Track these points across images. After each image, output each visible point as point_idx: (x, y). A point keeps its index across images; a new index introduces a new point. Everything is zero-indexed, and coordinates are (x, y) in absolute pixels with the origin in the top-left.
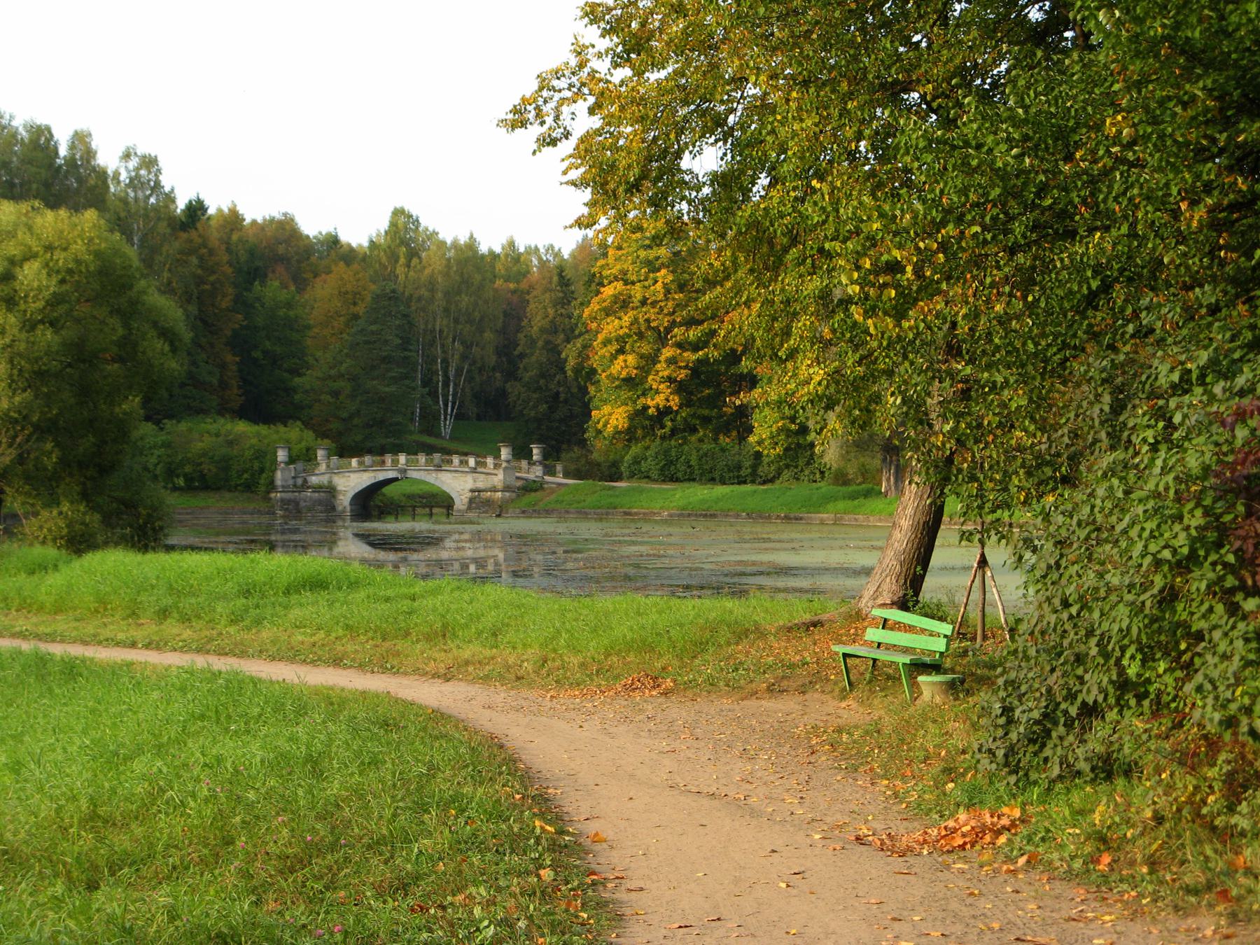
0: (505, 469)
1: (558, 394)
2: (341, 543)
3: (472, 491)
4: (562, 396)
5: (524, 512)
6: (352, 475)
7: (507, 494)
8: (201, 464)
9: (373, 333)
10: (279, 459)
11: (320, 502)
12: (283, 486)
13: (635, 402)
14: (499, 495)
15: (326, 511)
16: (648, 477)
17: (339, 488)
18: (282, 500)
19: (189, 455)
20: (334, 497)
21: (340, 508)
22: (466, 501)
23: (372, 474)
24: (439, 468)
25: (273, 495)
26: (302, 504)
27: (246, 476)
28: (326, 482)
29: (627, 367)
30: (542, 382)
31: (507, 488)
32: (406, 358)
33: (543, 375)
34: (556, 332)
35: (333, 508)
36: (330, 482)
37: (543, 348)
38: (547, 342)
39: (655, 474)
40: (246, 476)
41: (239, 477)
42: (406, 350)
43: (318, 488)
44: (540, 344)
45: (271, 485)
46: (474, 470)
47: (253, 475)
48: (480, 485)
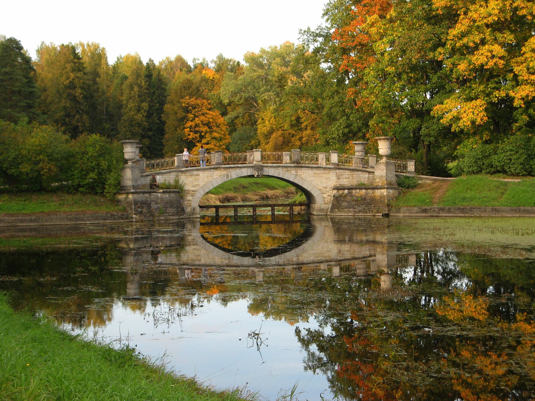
1: (77, 126)
2: (189, 249)
3: (338, 188)
4: (81, 128)
5: (425, 211)
6: (201, 173)
7: (391, 191)
8: (37, 163)
9: (6, 73)
10: (126, 156)
11: (171, 204)
12: (134, 187)
13: (488, 95)
14: (378, 192)
15: (177, 214)
16: (504, 172)
17: (187, 188)
18: (136, 202)
19: (24, 152)
20: (182, 198)
21: (188, 210)
23: (224, 172)
24: (298, 164)
25: (122, 197)
26: (154, 206)
27: (92, 175)
28: (172, 182)
29: (493, 57)
30: (67, 119)
31: (390, 186)
32: (31, 93)
33: (68, 115)
34: (75, 88)
35: (183, 210)
36: (177, 181)
37: (66, 98)
38: (69, 95)
39: (516, 167)
40: (92, 175)
41: (84, 177)
42: (30, 87)
43: (167, 189)
44: (65, 95)
45: (120, 188)
46: (337, 167)
47: (100, 174)
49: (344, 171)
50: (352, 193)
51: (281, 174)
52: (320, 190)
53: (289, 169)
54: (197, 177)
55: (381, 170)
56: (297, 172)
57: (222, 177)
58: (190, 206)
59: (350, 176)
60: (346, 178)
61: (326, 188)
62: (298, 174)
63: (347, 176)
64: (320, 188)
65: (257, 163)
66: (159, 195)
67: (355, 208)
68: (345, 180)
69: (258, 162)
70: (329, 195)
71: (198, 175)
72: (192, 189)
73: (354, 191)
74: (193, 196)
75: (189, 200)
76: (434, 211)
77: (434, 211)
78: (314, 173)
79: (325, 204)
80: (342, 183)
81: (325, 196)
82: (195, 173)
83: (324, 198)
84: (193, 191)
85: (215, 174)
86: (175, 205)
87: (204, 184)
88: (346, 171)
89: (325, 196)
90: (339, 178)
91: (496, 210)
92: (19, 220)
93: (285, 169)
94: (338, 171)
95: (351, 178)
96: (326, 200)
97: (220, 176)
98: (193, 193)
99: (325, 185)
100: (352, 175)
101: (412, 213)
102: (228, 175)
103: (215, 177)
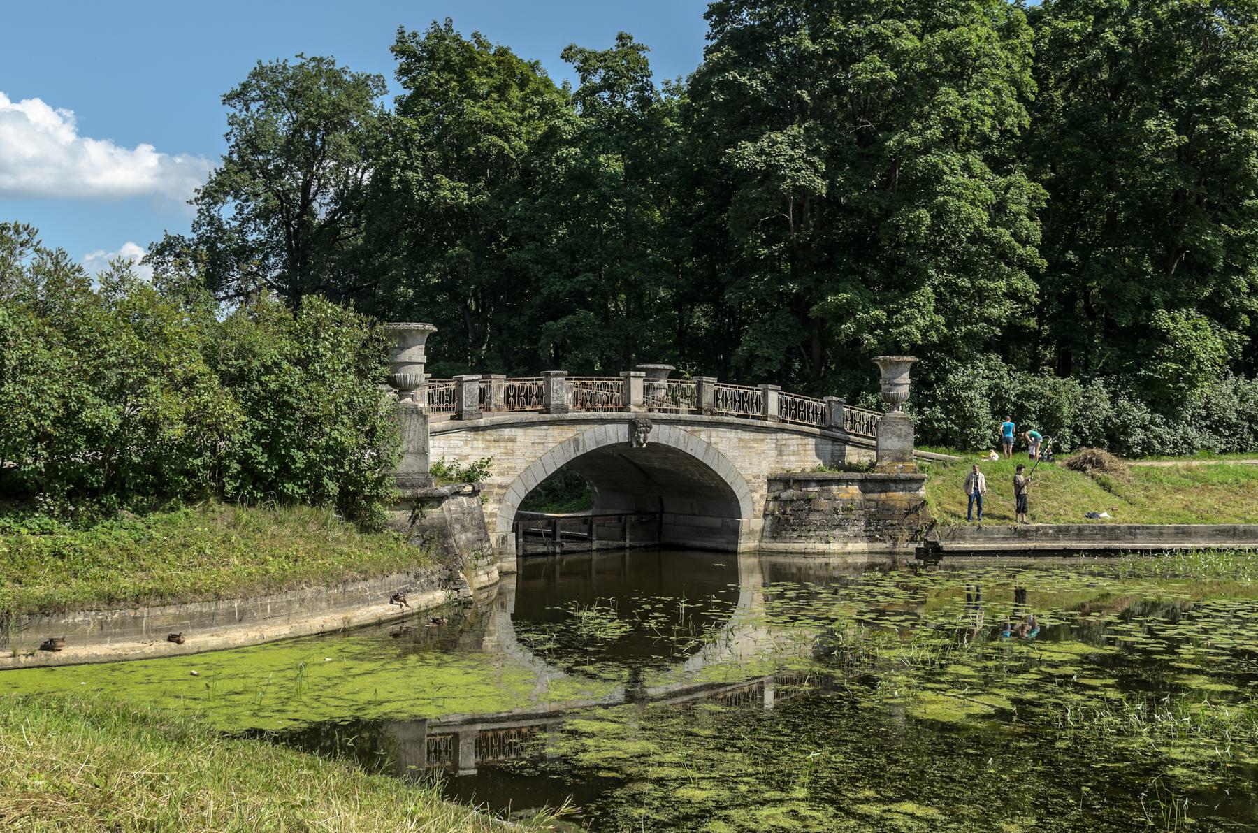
6: (518, 433)
24: (702, 416)
49: (791, 436)
50: (829, 491)
51: (681, 438)
52: (748, 482)
53: (697, 428)
54: (510, 445)
55: (899, 436)
56: (710, 437)
57: (565, 445)
62: (713, 440)
65: (637, 409)
67: (846, 530)
68: (792, 458)
71: (513, 440)
73: (834, 488)
76: (1046, 534)
77: (1046, 534)
78: (740, 440)
79: (756, 517)
80: (787, 465)
82: (507, 432)
84: (500, 487)
85: (550, 439)
87: (524, 466)
88: (795, 436)
89: (756, 496)
90: (780, 453)
91: (1184, 533)
92: (191, 616)
93: (689, 428)
94: (779, 436)
97: (560, 443)
98: (502, 491)
99: (756, 471)
100: (805, 445)
101: (993, 539)
102: (576, 441)
103: (551, 446)
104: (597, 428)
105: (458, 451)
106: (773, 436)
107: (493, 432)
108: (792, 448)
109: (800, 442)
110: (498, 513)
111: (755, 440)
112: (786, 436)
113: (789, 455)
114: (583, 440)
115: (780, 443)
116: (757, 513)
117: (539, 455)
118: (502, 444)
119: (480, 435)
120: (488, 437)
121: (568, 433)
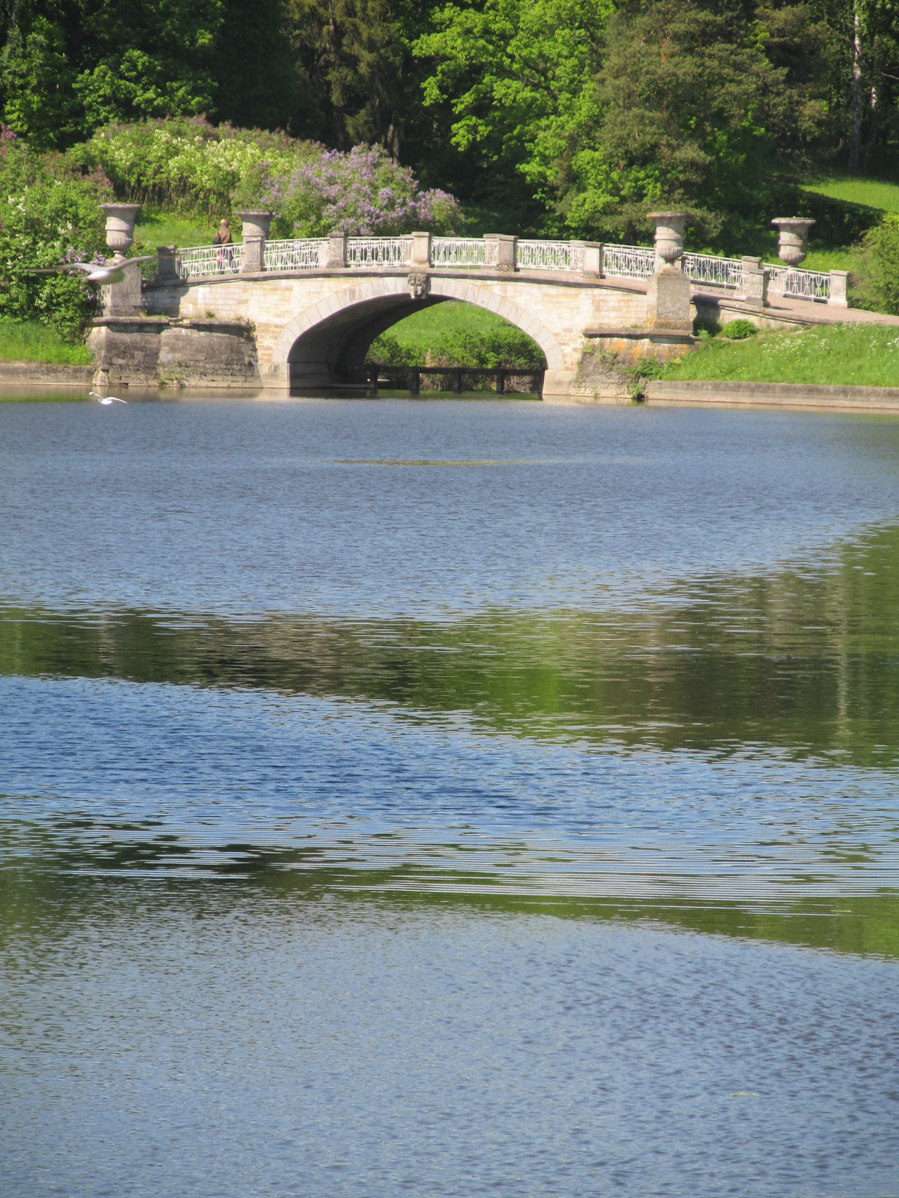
0: (664, 277)
22: (578, 356)
48: (613, 320)
51: (470, 292)
52: (555, 335)
53: (489, 282)
54: (287, 293)
56: (505, 291)
58: (269, 361)
59: (622, 304)
60: (614, 309)
61: (570, 330)
62: (509, 294)
63: (617, 305)
64: (556, 331)
65: (416, 265)
66: (184, 331)
68: (613, 314)
69: (421, 262)
70: (575, 350)
71: (289, 289)
72: (277, 321)
74: (276, 338)
75: (268, 348)
78: (545, 295)
79: (567, 369)
80: (606, 321)
81: (568, 349)
82: (284, 283)
83: (564, 356)
84: (277, 326)
85: (325, 289)
86: (224, 357)
87: (300, 310)
88: (616, 292)
89: (568, 349)
90: (598, 309)
93: (479, 282)
94: (596, 291)
95: (625, 309)
96: (569, 360)
97: (337, 292)
98: (278, 330)
99: (566, 325)
100: (628, 301)
102: (352, 292)
103: (326, 295)
104: (374, 280)
105: (235, 297)
106: (589, 291)
107: (270, 282)
108: (611, 304)
109: (621, 298)
110: (274, 347)
111: (566, 295)
112: (604, 291)
113: (608, 311)
114: (360, 291)
115: (597, 299)
116: (569, 366)
117: (314, 302)
118: (279, 292)
119: (257, 285)
120: (266, 287)
121: (344, 284)
